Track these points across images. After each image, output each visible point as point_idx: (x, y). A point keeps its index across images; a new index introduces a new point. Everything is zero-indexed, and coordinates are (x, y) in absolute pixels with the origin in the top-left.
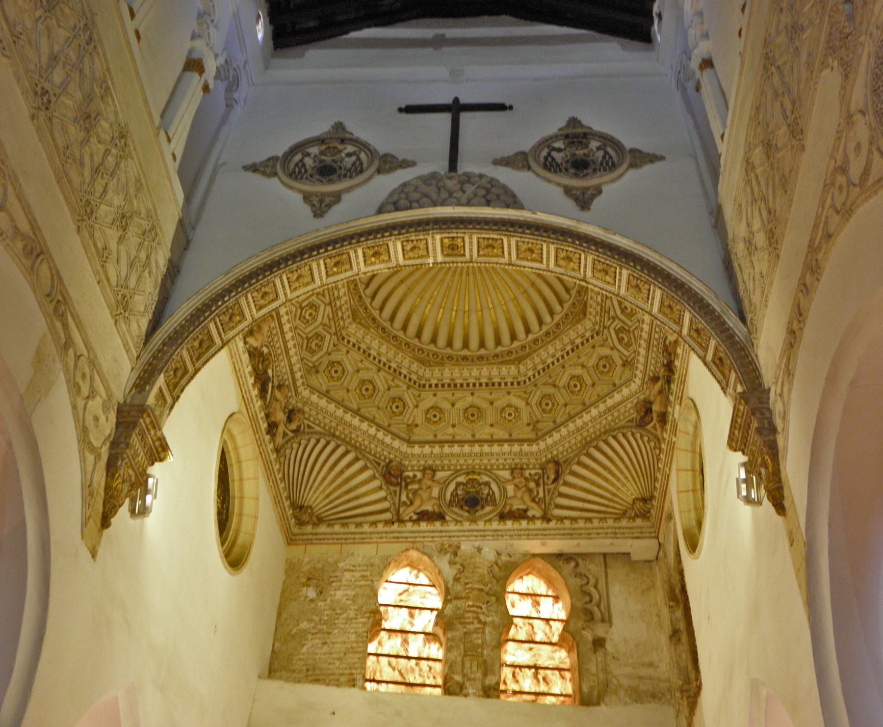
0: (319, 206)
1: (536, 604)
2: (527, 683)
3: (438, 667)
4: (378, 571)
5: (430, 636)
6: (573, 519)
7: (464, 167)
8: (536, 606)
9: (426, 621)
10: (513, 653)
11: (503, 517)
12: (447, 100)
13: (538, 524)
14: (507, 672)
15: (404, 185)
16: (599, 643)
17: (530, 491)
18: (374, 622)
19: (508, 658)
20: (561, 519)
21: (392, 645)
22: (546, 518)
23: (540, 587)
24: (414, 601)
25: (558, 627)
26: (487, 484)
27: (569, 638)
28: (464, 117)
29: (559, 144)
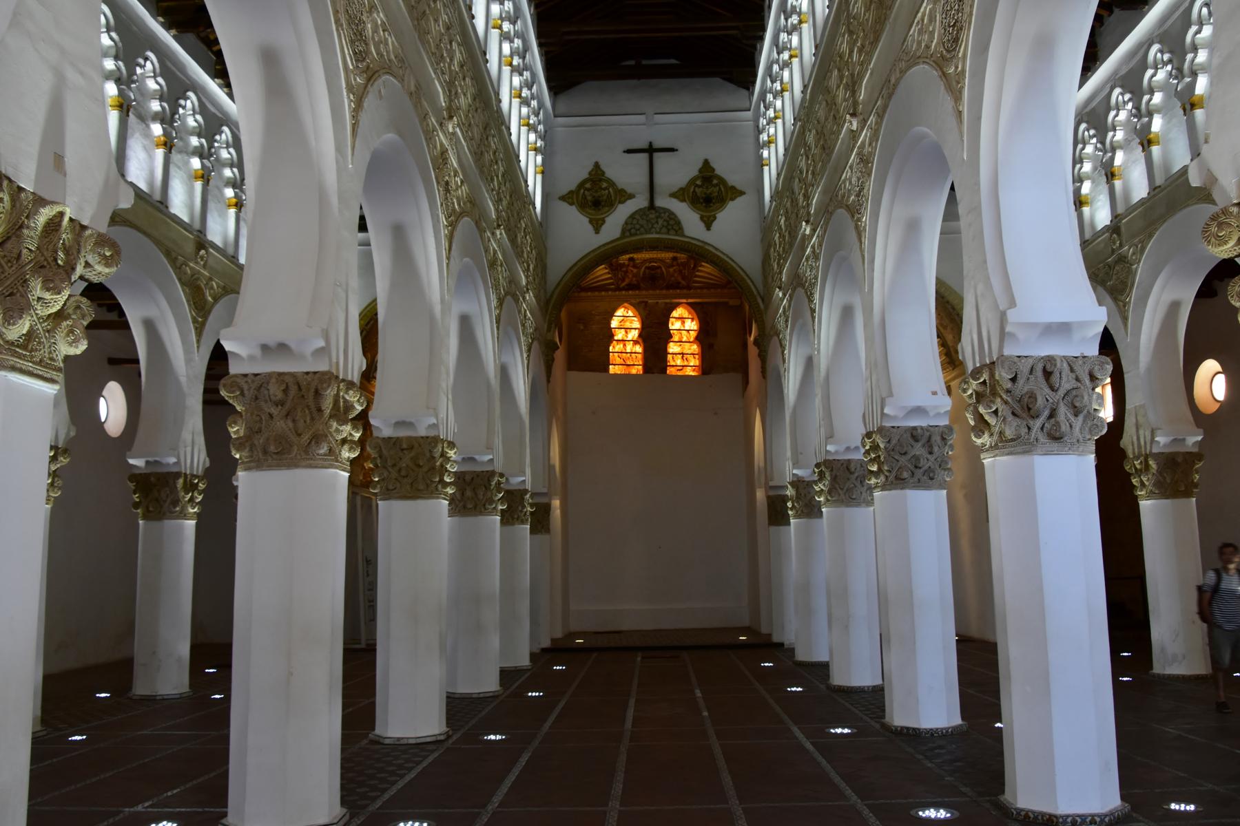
0: (597, 225)
1: (683, 323)
2: (679, 362)
3: (640, 356)
4: (611, 315)
5: (635, 342)
6: (701, 288)
7: (659, 202)
8: (683, 324)
9: (634, 334)
10: (673, 348)
11: (669, 287)
12: (645, 145)
13: (685, 291)
14: (670, 357)
15: (632, 216)
16: (711, 346)
17: (680, 271)
18: (609, 336)
19: (670, 350)
20: (696, 288)
21: (619, 347)
22: (689, 288)
23: (686, 314)
24: (628, 325)
25: (693, 334)
26: (659, 267)
27: (699, 339)
28: (656, 155)
29: (698, 182)
